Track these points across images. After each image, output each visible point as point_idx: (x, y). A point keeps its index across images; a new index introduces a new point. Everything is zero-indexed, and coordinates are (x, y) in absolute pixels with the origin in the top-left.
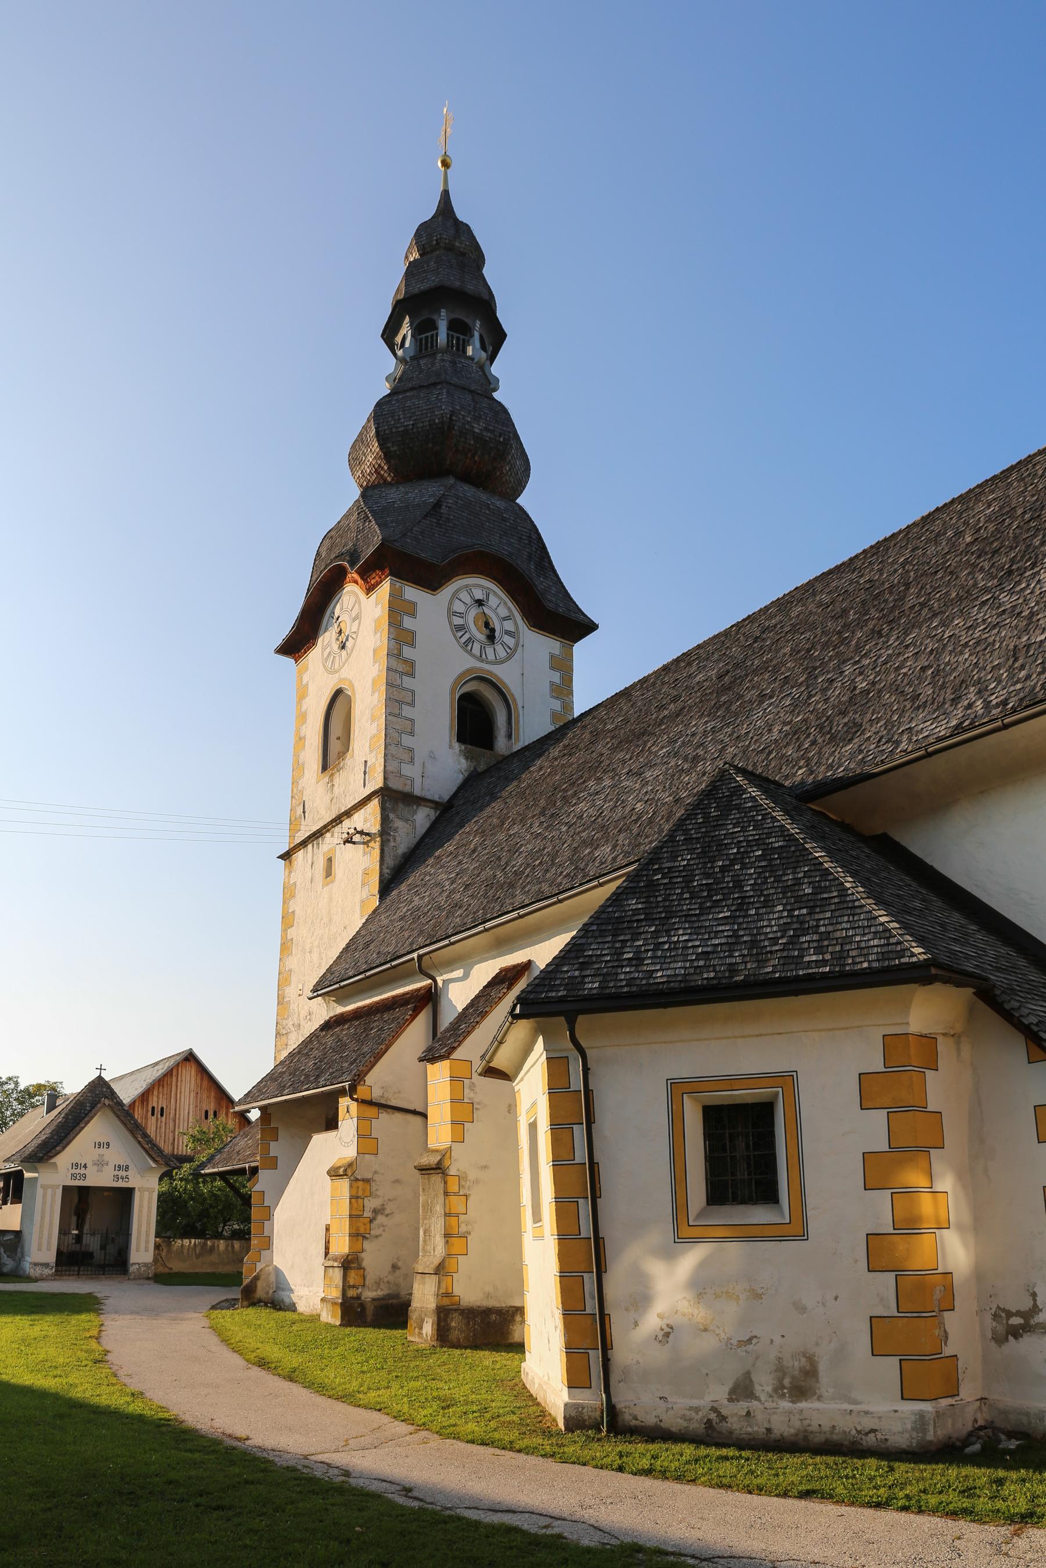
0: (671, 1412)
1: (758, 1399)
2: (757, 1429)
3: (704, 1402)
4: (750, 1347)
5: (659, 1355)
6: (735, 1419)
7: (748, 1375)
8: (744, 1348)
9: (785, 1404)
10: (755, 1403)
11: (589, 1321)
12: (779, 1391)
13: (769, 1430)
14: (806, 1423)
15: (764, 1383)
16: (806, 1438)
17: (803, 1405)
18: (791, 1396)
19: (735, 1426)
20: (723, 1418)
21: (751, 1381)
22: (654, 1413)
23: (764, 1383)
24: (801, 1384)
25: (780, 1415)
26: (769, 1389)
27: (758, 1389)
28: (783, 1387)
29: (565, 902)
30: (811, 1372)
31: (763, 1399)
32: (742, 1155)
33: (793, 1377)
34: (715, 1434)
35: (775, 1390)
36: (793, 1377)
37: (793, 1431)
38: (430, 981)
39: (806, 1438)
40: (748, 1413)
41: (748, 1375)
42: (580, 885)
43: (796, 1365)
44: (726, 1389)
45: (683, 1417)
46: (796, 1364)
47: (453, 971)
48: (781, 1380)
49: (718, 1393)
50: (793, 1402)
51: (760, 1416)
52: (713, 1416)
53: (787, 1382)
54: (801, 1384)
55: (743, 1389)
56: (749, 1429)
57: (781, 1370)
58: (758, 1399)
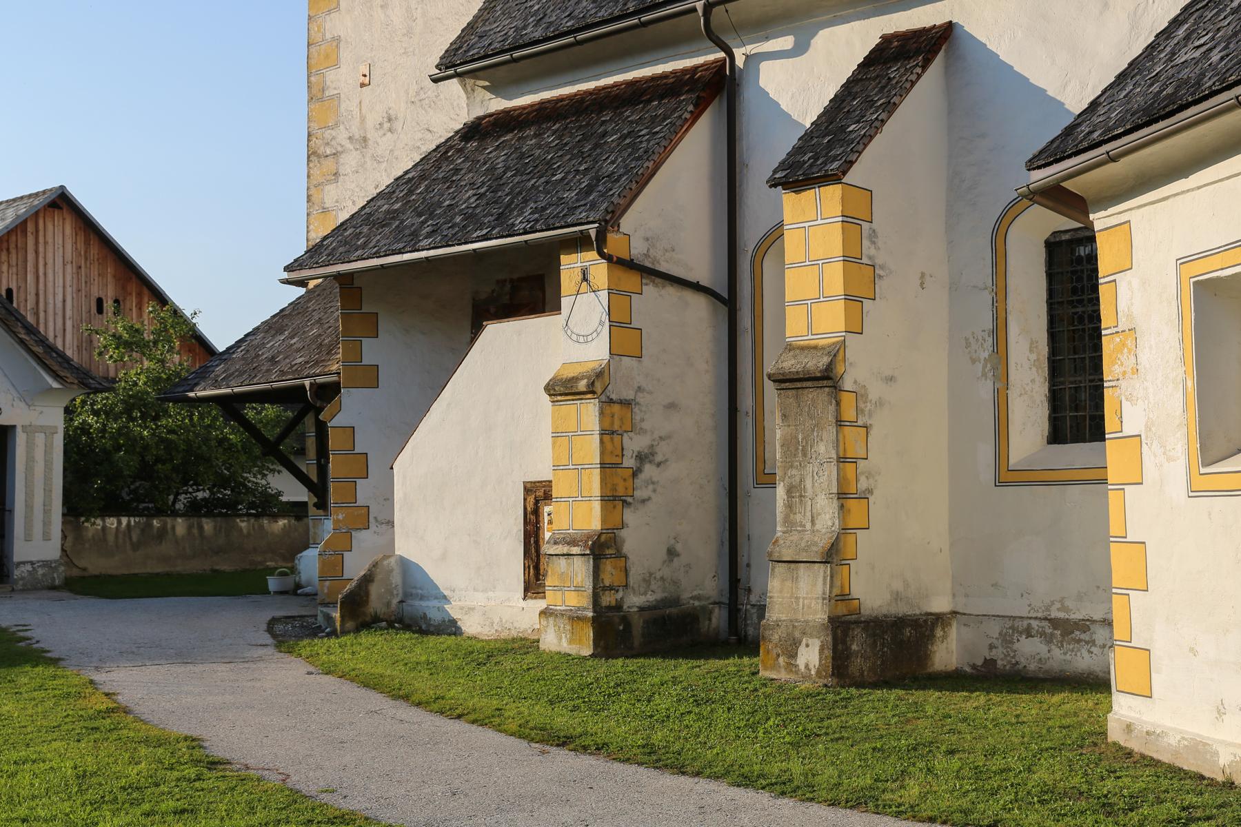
38: (722, 55)
47: (767, 39)
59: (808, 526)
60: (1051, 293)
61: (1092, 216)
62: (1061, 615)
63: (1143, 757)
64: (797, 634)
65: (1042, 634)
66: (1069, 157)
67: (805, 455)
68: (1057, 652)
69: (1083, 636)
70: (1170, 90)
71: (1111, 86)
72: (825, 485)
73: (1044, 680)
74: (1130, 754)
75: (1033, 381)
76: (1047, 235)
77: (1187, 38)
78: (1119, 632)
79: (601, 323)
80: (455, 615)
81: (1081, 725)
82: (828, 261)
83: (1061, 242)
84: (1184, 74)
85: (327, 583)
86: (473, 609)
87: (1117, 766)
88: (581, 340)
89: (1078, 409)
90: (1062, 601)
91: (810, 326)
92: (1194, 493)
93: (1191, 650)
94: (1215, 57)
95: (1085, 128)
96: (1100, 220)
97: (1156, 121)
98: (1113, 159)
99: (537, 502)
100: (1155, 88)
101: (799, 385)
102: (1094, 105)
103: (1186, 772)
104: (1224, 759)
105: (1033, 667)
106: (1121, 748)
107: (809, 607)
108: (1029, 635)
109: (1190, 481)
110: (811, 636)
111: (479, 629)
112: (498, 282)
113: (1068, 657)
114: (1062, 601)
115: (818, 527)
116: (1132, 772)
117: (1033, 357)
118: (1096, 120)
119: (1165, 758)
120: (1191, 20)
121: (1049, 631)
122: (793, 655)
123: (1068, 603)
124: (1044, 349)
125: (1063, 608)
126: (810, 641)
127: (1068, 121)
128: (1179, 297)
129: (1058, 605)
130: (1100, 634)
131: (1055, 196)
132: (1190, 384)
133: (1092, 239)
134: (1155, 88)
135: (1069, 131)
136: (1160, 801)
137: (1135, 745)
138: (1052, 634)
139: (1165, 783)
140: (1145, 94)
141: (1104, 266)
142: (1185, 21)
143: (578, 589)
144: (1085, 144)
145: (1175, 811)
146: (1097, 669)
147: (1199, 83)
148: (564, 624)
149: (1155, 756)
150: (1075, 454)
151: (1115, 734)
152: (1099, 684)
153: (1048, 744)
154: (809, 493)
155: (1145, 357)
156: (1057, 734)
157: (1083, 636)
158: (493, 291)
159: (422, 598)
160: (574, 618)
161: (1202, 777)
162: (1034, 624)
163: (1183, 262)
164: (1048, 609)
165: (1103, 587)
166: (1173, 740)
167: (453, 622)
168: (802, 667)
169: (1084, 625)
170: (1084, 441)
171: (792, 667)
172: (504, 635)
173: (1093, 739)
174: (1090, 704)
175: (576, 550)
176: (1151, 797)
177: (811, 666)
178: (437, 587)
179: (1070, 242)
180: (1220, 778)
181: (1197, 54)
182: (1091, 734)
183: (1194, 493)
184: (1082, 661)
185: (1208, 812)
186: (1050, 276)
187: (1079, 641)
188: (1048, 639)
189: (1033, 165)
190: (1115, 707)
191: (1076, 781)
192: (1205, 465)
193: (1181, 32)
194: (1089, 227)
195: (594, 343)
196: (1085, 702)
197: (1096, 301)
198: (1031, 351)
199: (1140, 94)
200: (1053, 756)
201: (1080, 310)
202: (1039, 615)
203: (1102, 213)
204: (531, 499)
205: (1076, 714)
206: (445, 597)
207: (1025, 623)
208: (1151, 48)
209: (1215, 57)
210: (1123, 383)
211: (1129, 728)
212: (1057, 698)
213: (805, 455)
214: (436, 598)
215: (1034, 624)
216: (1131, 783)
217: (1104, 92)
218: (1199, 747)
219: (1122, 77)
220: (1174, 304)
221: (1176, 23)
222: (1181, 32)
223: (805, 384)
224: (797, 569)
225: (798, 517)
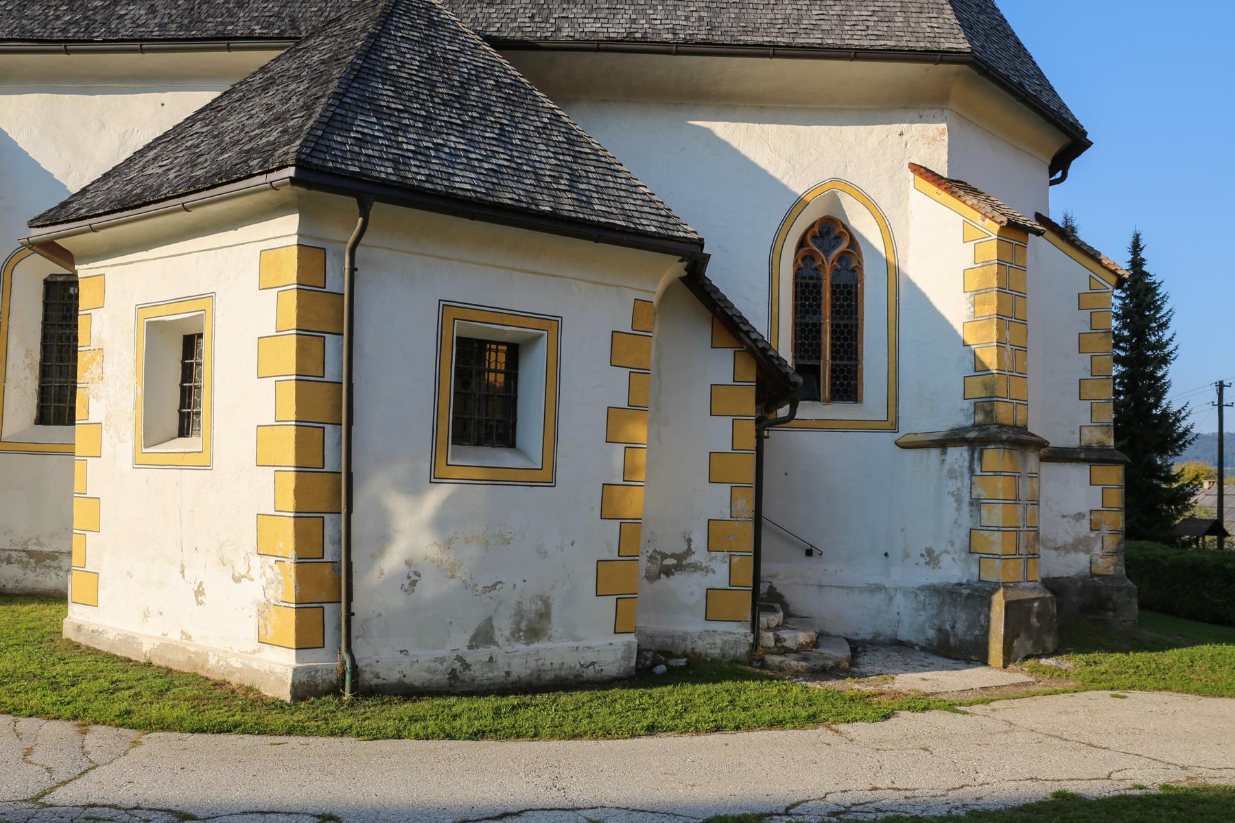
0: (416, 666)
1: (496, 644)
2: (497, 674)
3: (446, 652)
4: (494, 593)
5: (398, 600)
6: (478, 666)
7: (489, 622)
8: (488, 594)
9: (520, 647)
10: (494, 648)
11: (327, 570)
12: (515, 635)
13: (508, 673)
14: (540, 662)
15: (503, 628)
16: (539, 677)
17: (535, 646)
18: (526, 637)
19: (478, 673)
20: (467, 666)
21: (492, 627)
22: (399, 669)
23: (503, 628)
24: (534, 627)
25: (517, 658)
26: (507, 633)
27: (497, 636)
28: (520, 630)
29: (72, 56)
30: (544, 615)
31: (501, 643)
32: (484, 398)
33: (529, 621)
34: (458, 684)
35: (513, 634)
36: (529, 621)
37: (528, 672)
39: (539, 677)
40: (491, 659)
41: (489, 622)
42: (104, 41)
43: (532, 608)
44: (468, 636)
45: (428, 670)
46: (533, 607)
48: (518, 624)
49: (459, 642)
50: (527, 644)
51: (501, 661)
52: (457, 665)
53: (523, 625)
54: (534, 627)
55: (484, 636)
56: (490, 675)
57: (519, 614)
58: (496, 644)
60: (46, 317)
61: (76, 267)
62: (36, 548)
63: (88, 648)
65: (20, 562)
66: (62, 223)
68: (31, 575)
69: (52, 564)
70: (138, 191)
71: (98, 180)
73: (19, 595)
74: (78, 646)
75: (26, 378)
76: (46, 276)
77: (155, 159)
78: (76, 560)
81: (44, 627)
83: (56, 282)
84: (150, 182)
87: (66, 655)
89: (57, 402)
90: (37, 538)
92: (138, 465)
93: (128, 573)
94: (172, 175)
95: (76, 205)
96: (82, 270)
97: (127, 209)
98: (94, 230)
100: (129, 187)
102: (84, 191)
103: (118, 658)
104: (146, 648)
105: (10, 586)
106: (72, 642)
108: (9, 562)
109: (135, 458)
113: (40, 578)
114: (37, 538)
116: (78, 659)
117: (28, 361)
118: (84, 201)
119: (104, 648)
120: (159, 148)
121: (25, 559)
123: (42, 540)
124: (37, 357)
125: (38, 543)
127: (65, 198)
128: (136, 331)
129: (34, 541)
130: (64, 563)
131: (50, 248)
132: (139, 391)
133: (75, 284)
134: (129, 187)
135: (64, 205)
136: (95, 678)
137: (82, 640)
138: (28, 563)
139: (101, 665)
140: (121, 190)
141: (83, 303)
142: (155, 148)
144: (74, 216)
145: (106, 685)
146: (61, 587)
147: (158, 190)
149: (97, 647)
150: (54, 433)
151: (68, 632)
152: (59, 597)
153: (14, 642)
155: (108, 369)
156: (23, 634)
157: (52, 564)
161: (130, 660)
162: (14, 554)
163: (140, 307)
164: (26, 543)
165: (67, 529)
166: (111, 636)
169: (54, 556)
170: (64, 424)
173: (52, 637)
174: (53, 612)
176: (89, 675)
179: (63, 283)
180: (143, 661)
181: (160, 171)
182: (50, 633)
183: (138, 465)
184: (49, 581)
185: (130, 684)
186: (47, 305)
187: (49, 567)
188: (25, 565)
189: (34, 223)
190: (70, 614)
191: (34, 667)
192: (146, 447)
193: (151, 154)
194: (75, 274)
196: (48, 610)
197: (76, 326)
198: (26, 357)
199: (118, 189)
200: (17, 650)
201: (67, 331)
202: (19, 548)
203: (85, 266)
205: (40, 619)
207: (7, 554)
208: (130, 160)
209: (172, 175)
210: (91, 386)
211: (79, 628)
212: (27, 608)
215: (14, 554)
216: (74, 668)
217: (93, 183)
218: (129, 640)
219: (106, 176)
220: (132, 335)
221: (149, 147)
222: (151, 154)
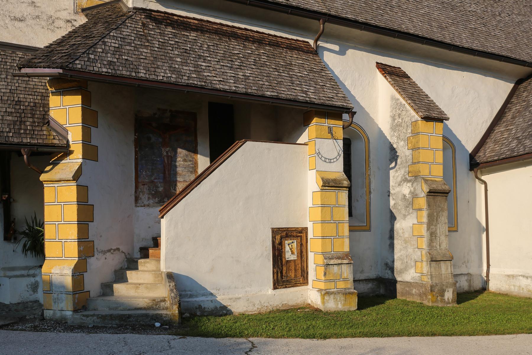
59: (438, 247)
64: (444, 288)
67: (437, 221)
72: (444, 232)
79: (339, 155)
80: (225, 303)
82: (437, 150)
85: (77, 296)
86: (240, 298)
88: (327, 161)
91: (430, 172)
99: (281, 238)
101: (436, 194)
107: (446, 277)
110: (450, 287)
111: (245, 309)
112: (159, 109)
115: (442, 247)
122: (443, 296)
126: (449, 290)
143: (345, 280)
148: (340, 297)
154: (438, 235)
158: (155, 114)
159: (191, 296)
160: (346, 294)
167: (225, 308)
168: (446, 300)
171: (443, 301)
172: (263, 310)
175: (345, 261)
177: (450, 299)
178: (204, 289)
195: (335, 163)
204: (278, 237)
206: (212, 294)
213: (437, 221)
214: (203, 295)
223: (438, 194)
224: (440, 263)
225: (434, 244)
